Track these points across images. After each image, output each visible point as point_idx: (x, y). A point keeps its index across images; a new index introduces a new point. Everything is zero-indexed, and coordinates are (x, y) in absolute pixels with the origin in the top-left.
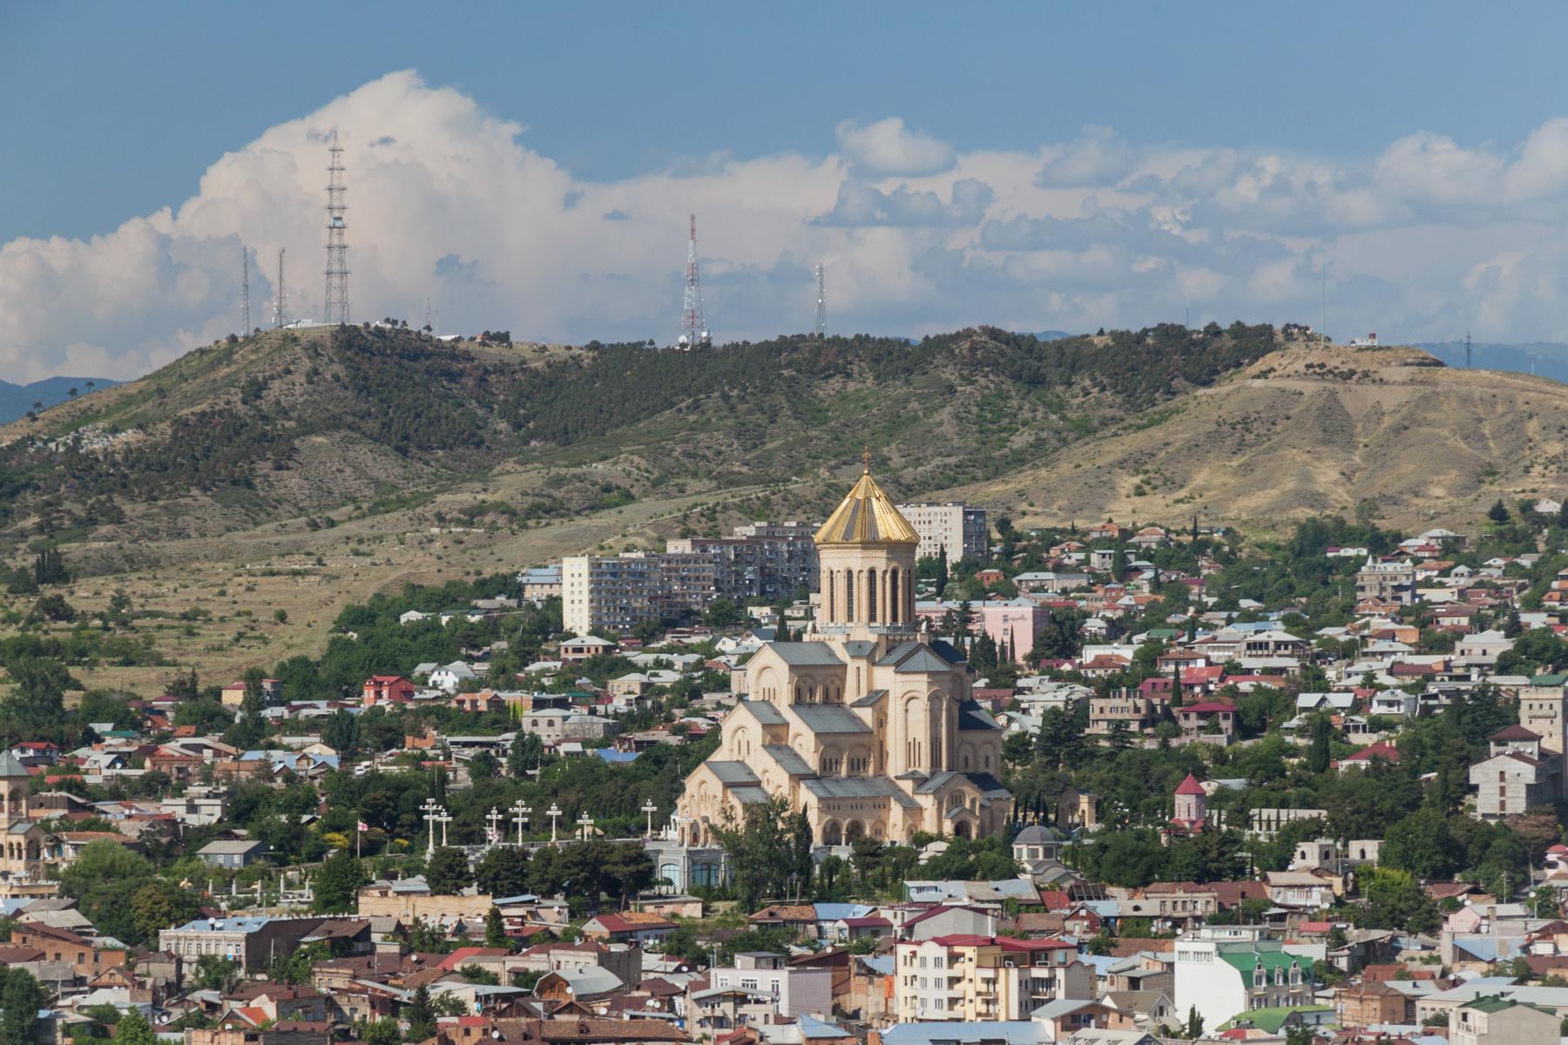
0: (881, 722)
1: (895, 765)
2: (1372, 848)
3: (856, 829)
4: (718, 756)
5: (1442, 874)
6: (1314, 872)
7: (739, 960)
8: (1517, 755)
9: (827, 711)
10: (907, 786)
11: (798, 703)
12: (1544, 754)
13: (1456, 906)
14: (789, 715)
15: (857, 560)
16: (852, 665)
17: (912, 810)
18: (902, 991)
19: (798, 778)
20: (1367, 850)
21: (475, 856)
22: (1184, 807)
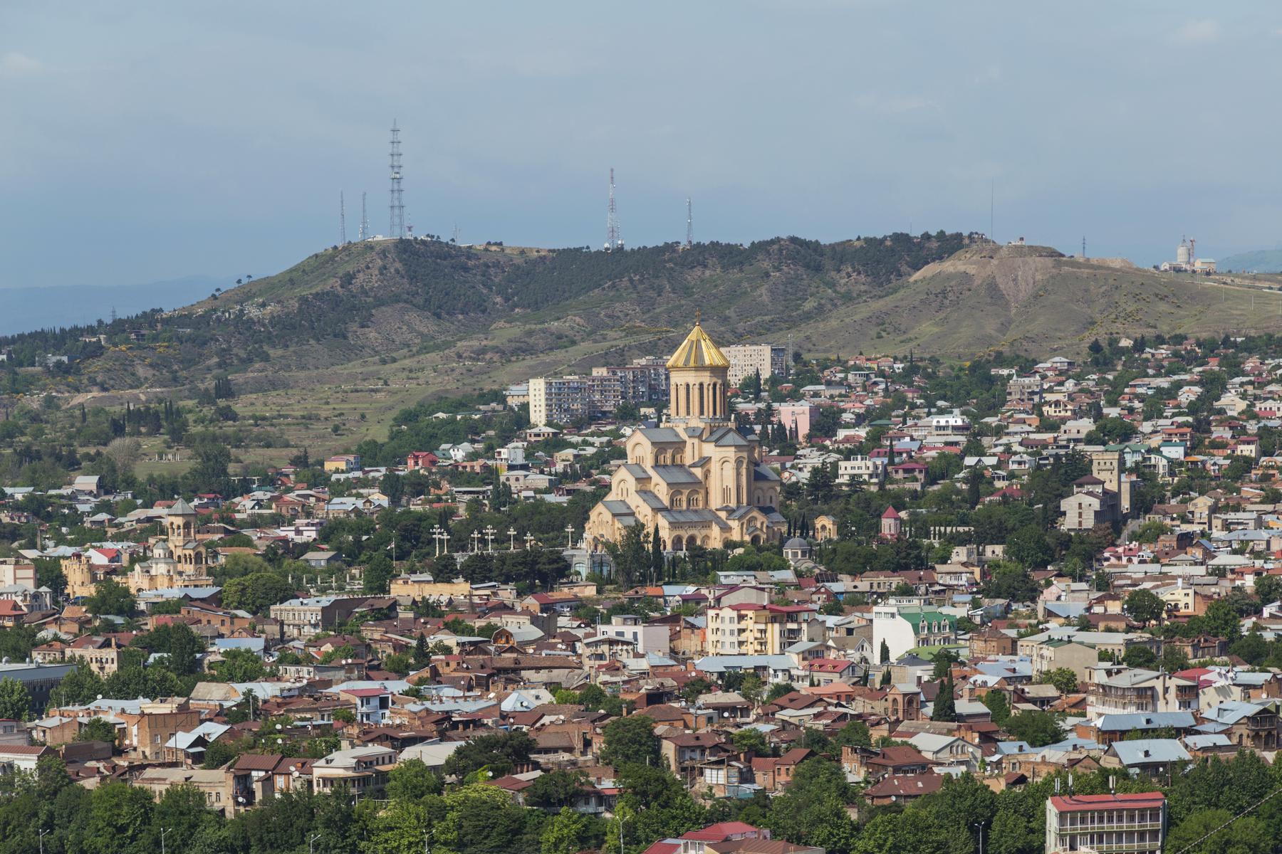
0: (706, 477)
1: (716, 502)
2: (999, 549)
3: (692, 539)
4: (609, 498)
5: (1042, 565)
6: (964, 564)
7: (614, 619)
8: (1090, 494)
9: (674, 470)
10: (723, 515)
11: (656, 466)
12: (1105, 492)
13: (1049, 584)
14: (651, 472)
15: (692, 378)
16: (689, 442)
17: (725, 528)
18: (711, 638)
19: (656, 510)
20: (995, 551)
21: (460, 558)
22: (888, 526)
